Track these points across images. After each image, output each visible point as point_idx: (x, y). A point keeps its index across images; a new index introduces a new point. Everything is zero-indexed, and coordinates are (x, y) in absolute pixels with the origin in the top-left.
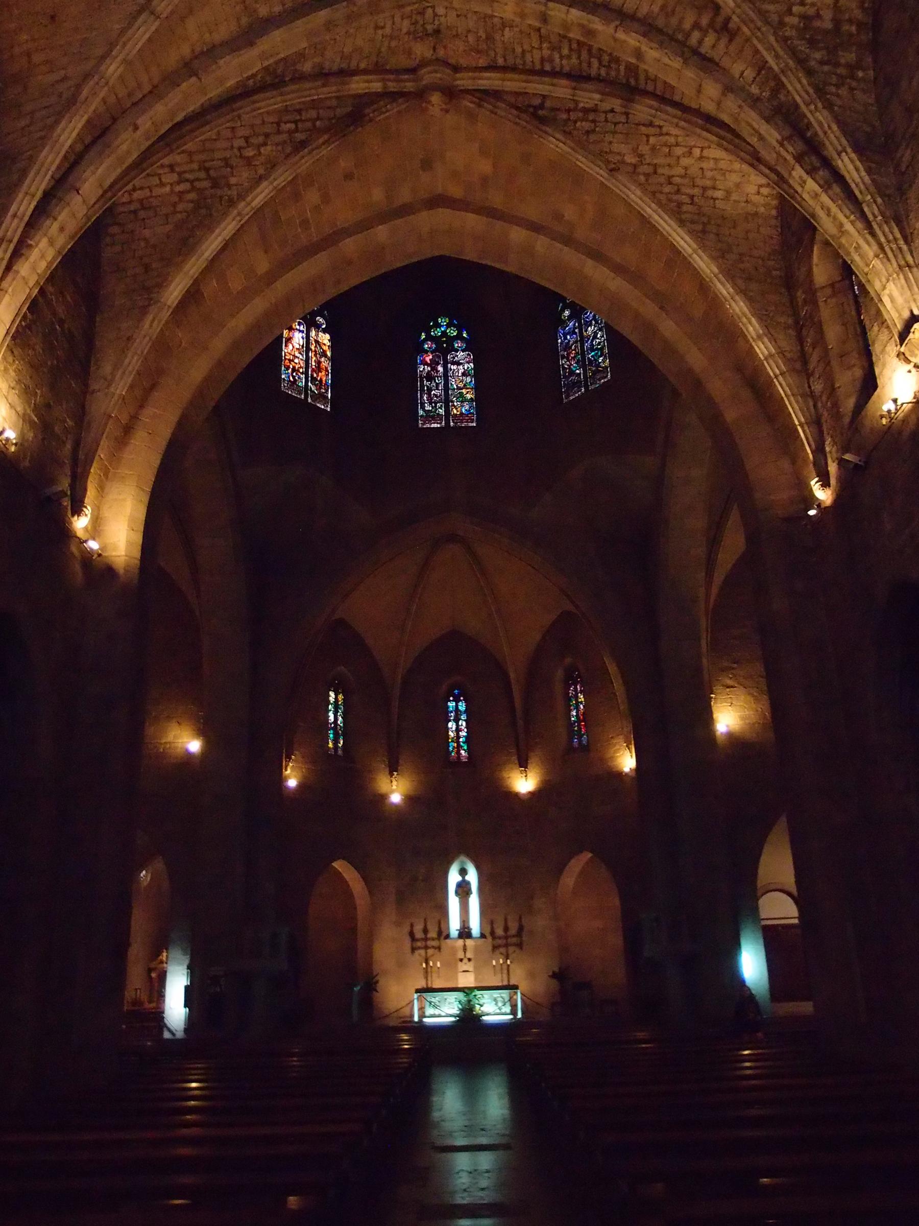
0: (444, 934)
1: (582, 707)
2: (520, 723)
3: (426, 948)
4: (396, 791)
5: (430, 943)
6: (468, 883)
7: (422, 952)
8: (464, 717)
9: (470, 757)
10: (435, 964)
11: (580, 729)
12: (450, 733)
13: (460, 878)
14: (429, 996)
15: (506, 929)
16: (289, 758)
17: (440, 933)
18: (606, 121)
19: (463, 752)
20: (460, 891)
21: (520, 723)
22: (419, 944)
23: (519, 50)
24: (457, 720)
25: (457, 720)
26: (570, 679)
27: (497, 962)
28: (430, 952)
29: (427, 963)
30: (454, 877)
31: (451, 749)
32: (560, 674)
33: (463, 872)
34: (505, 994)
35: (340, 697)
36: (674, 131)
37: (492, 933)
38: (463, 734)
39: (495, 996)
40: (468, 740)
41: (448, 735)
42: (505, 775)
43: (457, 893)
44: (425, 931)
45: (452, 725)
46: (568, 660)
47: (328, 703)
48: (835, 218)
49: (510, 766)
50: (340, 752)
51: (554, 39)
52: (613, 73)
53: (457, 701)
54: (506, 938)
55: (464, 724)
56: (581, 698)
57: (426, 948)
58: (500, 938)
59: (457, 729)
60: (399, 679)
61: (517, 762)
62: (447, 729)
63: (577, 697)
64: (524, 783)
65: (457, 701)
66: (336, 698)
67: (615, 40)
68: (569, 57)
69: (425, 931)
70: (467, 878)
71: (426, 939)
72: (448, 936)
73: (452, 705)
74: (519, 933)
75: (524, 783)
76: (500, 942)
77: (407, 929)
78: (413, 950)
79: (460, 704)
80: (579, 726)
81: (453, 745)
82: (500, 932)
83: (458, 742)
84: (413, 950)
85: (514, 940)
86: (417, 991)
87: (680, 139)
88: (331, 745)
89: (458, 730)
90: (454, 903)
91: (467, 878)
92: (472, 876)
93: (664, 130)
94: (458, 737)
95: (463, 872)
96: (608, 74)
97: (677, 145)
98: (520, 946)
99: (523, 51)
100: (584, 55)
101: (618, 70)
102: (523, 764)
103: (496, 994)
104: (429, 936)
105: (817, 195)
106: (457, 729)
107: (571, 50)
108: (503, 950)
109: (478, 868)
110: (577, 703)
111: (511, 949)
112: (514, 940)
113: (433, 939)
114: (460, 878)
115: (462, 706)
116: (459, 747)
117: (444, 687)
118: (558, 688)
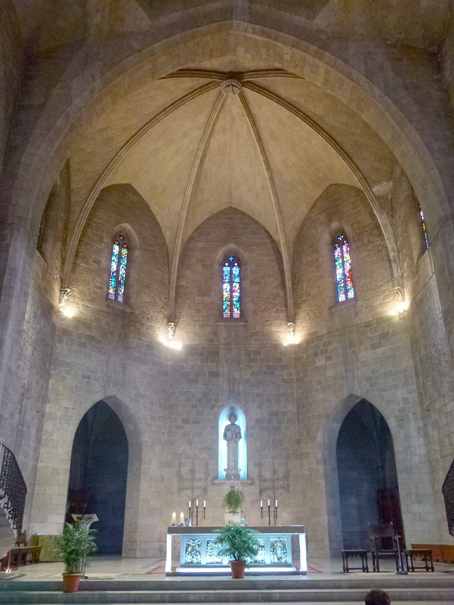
0: (212, 476)
1: (348, 264)
2: (288, 284)
3: (192, 489)
4: (172, 340)
5: (197, 484)
6: (238, 427)
7: (188, 492)
8: (237, 280)
9: (242, 314)
10: (201, 502)
11: (345, 286)
12: (225, 293)
13: (229, 423)
14: (184, 539)
15: (275, 472)
16: (63, 291)
17: (207, 474)
19: (235, 310)
20: (229, 434)
21: (288, 284)
22: (186, 484)
24: (231, 282)
25: (231, 282)
26: (335, 243)
27: (265, 502)
28: (197, 492)
29: (193, 502)
30: (224, 422)
31: (224, 307)
32: (326, 237)
33: (233, 417)
34: (286, 537)
35: (125, 252)
37: (260, 477)
38: (236, 294)
39: (272, 540)
40: (240, 300)
41: (222, 296)
42: (274, 329)
43: (225, 436)
44: (193, 472)
45: (226, 286)
46: (335, 225)
47: (112, 254)
49: (278, 322)
50: (120, 299)
53: (231, 265)
54: (273, 481)
55: (238, 285)
56: (347, 257)
57: (192, 489)
58: (265, 481)
59: (230, 290)
60: (179, 242)
61: (285, 318)
62: (222, 290)
63: (342, 257)
64: (291, 337)
65: (231, 265)
66: (120, 252)
69: (193, 472)
70: (236, 423)
71: (193, 480)
72: (216, 477)
73: (226, 270)
74: (286, 477)
75: (291, 337)
76: (266, 485)
77: (174, 471)
78: (180, 489)
79: (234, 269)
80: (345, 282)
81: (226, 304)
82: (267, 474)
83: (231, 300)
84: (180, 489)
85: (281, 483)
86: (171, 530)
88: (111, 291)
89: (232, 291)
90: (223, 445)
91: (236, 423)
92: (241, 422)
94: (232, 297)
95: (233, 417)
98: (287, 488)
102: (291, 319)
103: (273, 537)
104: (197, 476)
106: (230, 290)
108: (270, 493)
109: (246, 413)
110: (343, 262)
111: (278, 492)
112: (281, 483)
113: (200, 480)
114: (229, 423)
115: (236, 271)
116: (231, 305)
117: (220, 255)
118: (324, 250)
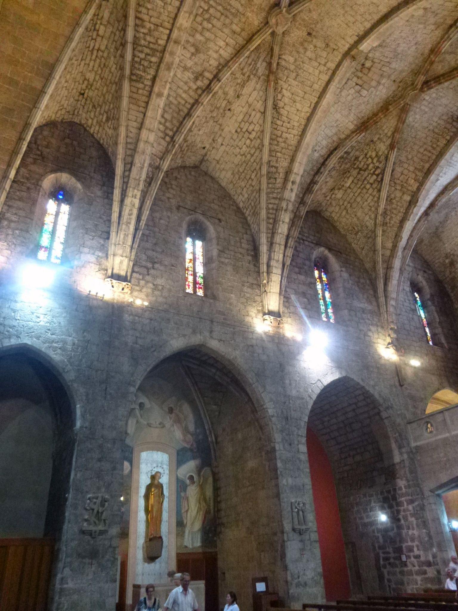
18: (89, 36)
23: (149, 6)
36: (77, 72)
48: (130, 219)
51: (156, 34)
52: (137, 65)
67: (166, 82)
68: (145, 40)
87: (73, 76)
93: (78, 67)
96: (136, 62)
97: (71, 75)
99: (148, 9)
100: (147, 50)
101: (139, 69)
105: (134, 205)
107: (149, 42)
